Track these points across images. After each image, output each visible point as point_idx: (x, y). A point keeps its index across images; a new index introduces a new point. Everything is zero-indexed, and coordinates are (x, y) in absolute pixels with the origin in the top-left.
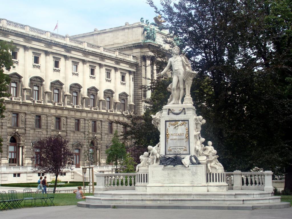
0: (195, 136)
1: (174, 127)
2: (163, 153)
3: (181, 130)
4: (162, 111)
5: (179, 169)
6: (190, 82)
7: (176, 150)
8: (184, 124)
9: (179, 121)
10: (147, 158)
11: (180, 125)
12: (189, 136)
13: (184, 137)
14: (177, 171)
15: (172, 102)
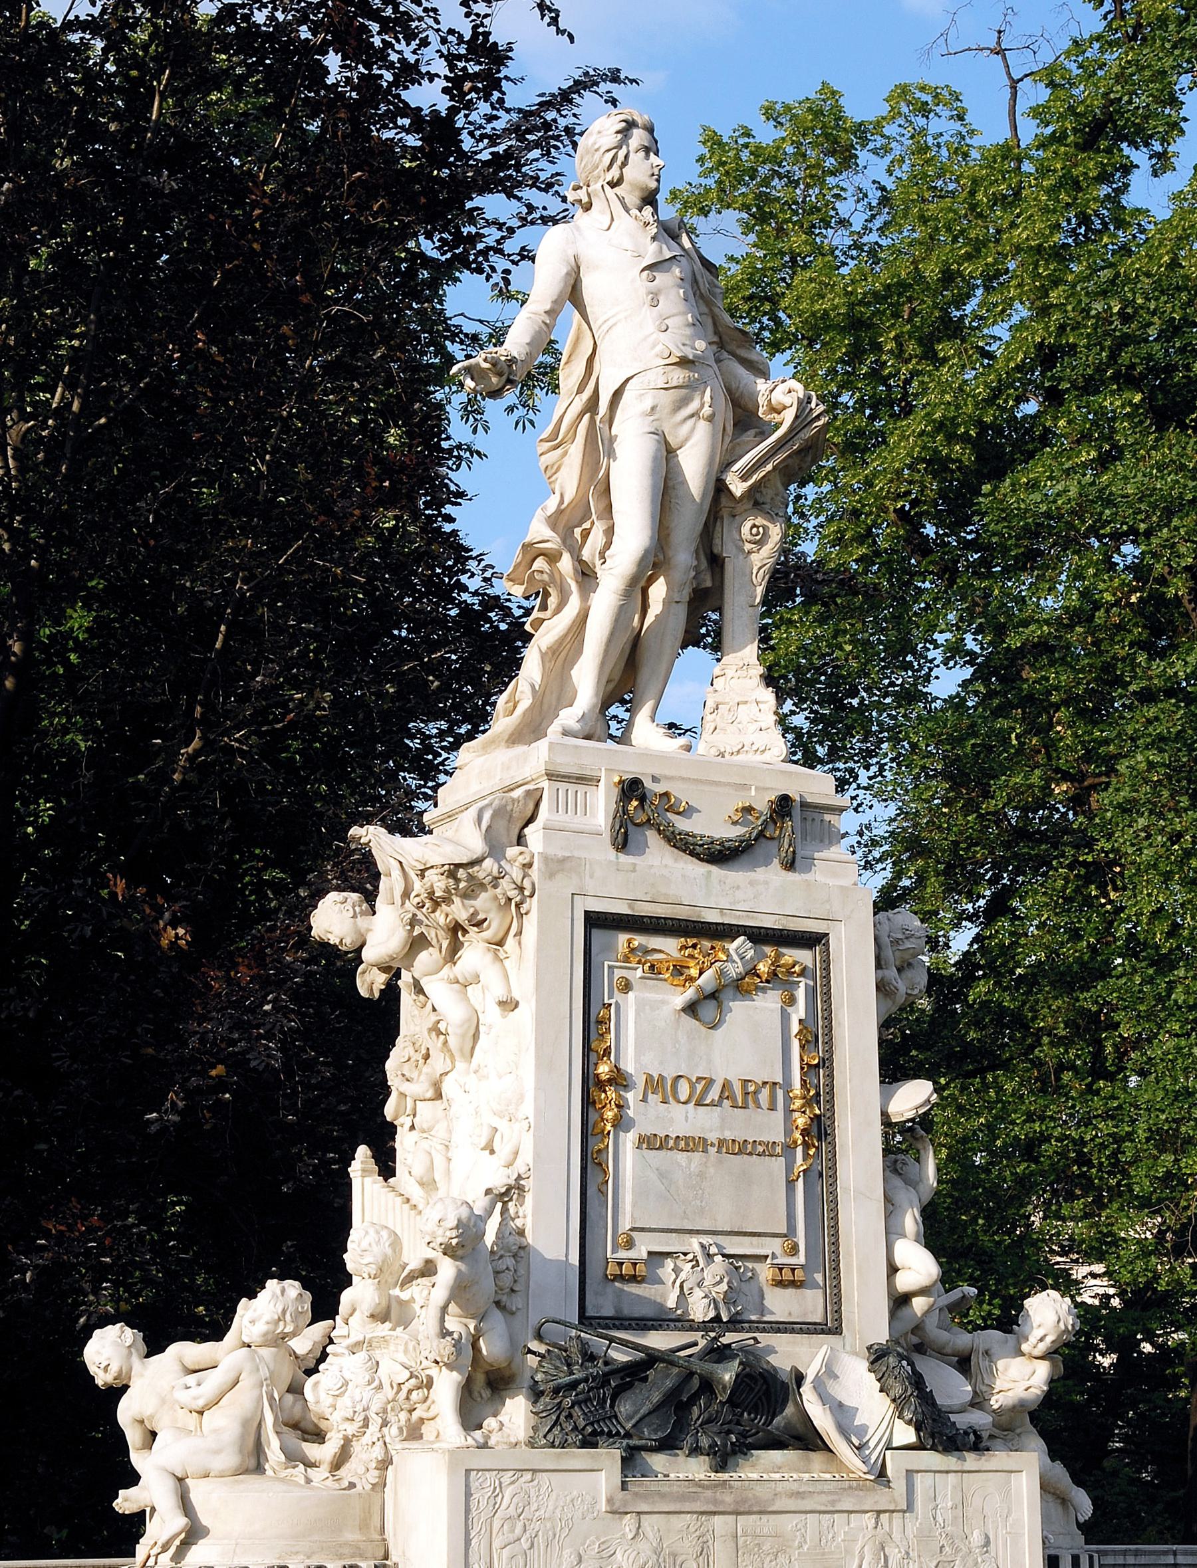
1: (690, 993)
5: (791, 1504)
14: (767, 1524)
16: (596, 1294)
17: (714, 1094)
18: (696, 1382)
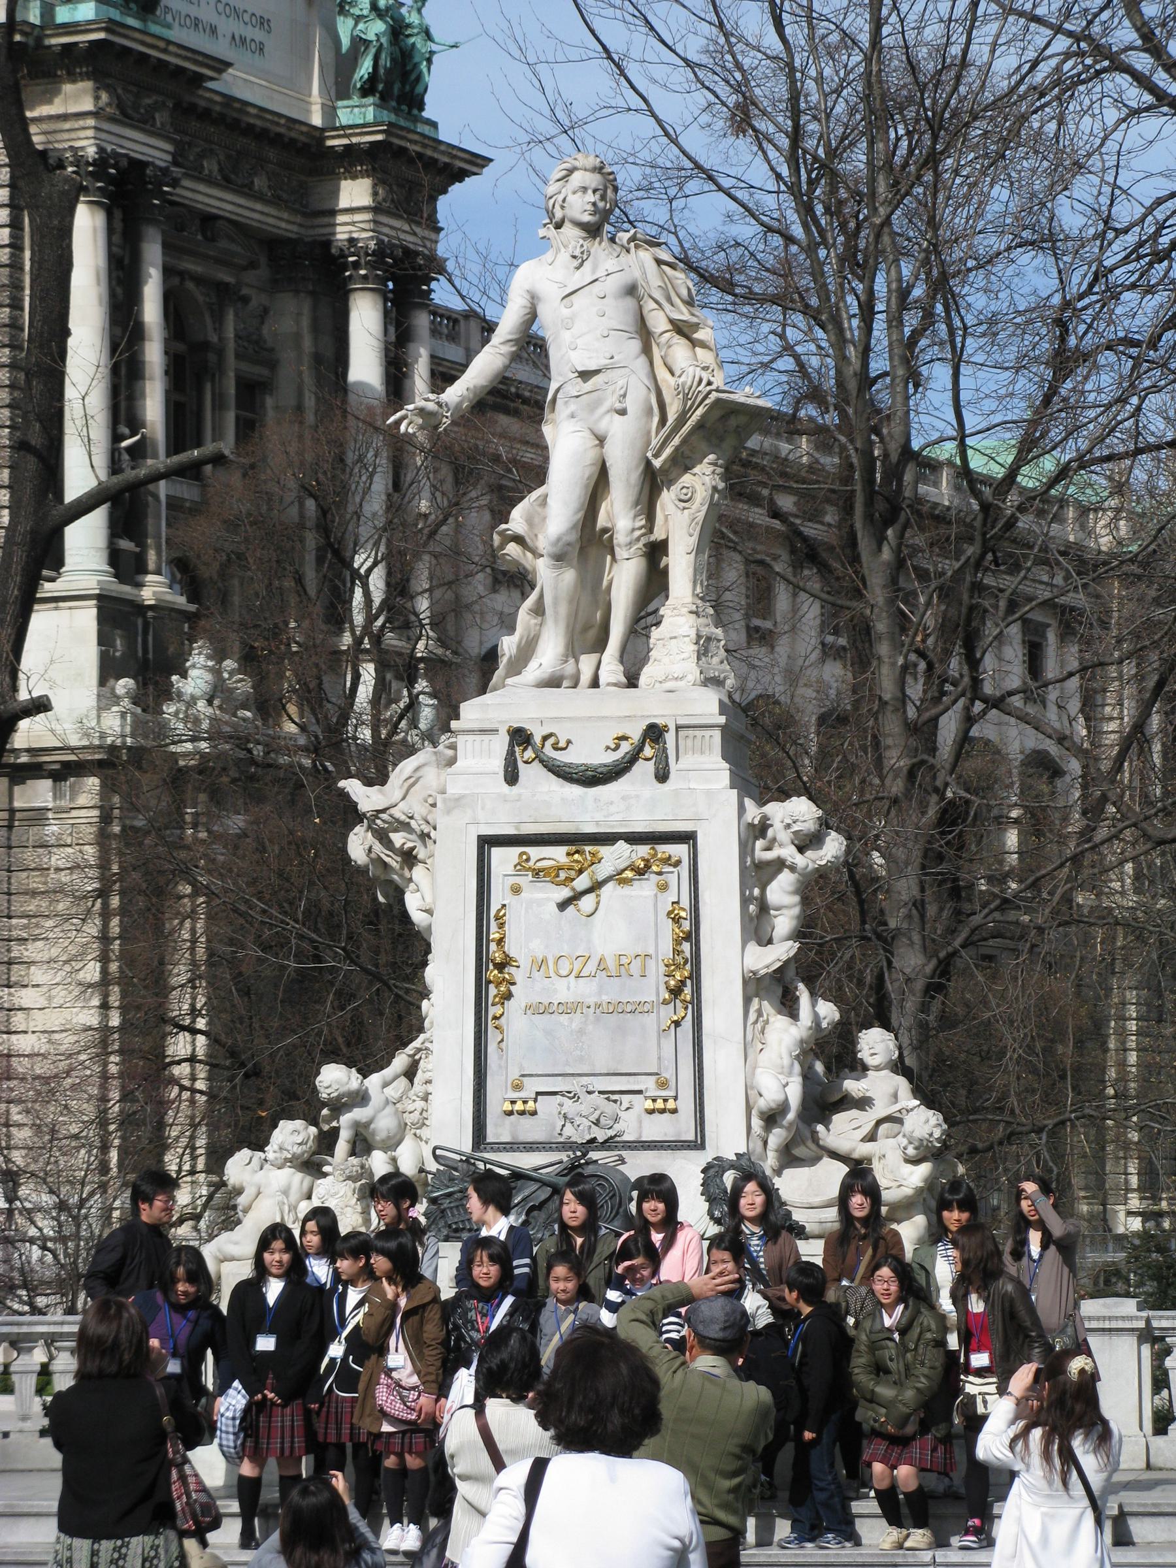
0: (754, 986)
1: (565, 893)
2: (450, 1128)
3: (628, 920)
4: (453, 747)
6: (703, 479)
7: (569, 1106)
8: (648, 866)
9: (608, 839)
10: (297, 1179)
11: (618, 878)
12: (696, 976)
13: (653, 987)
15: (534, 670)
16: (496, 1125)
17: (591, 967)
18: (548, 1191)
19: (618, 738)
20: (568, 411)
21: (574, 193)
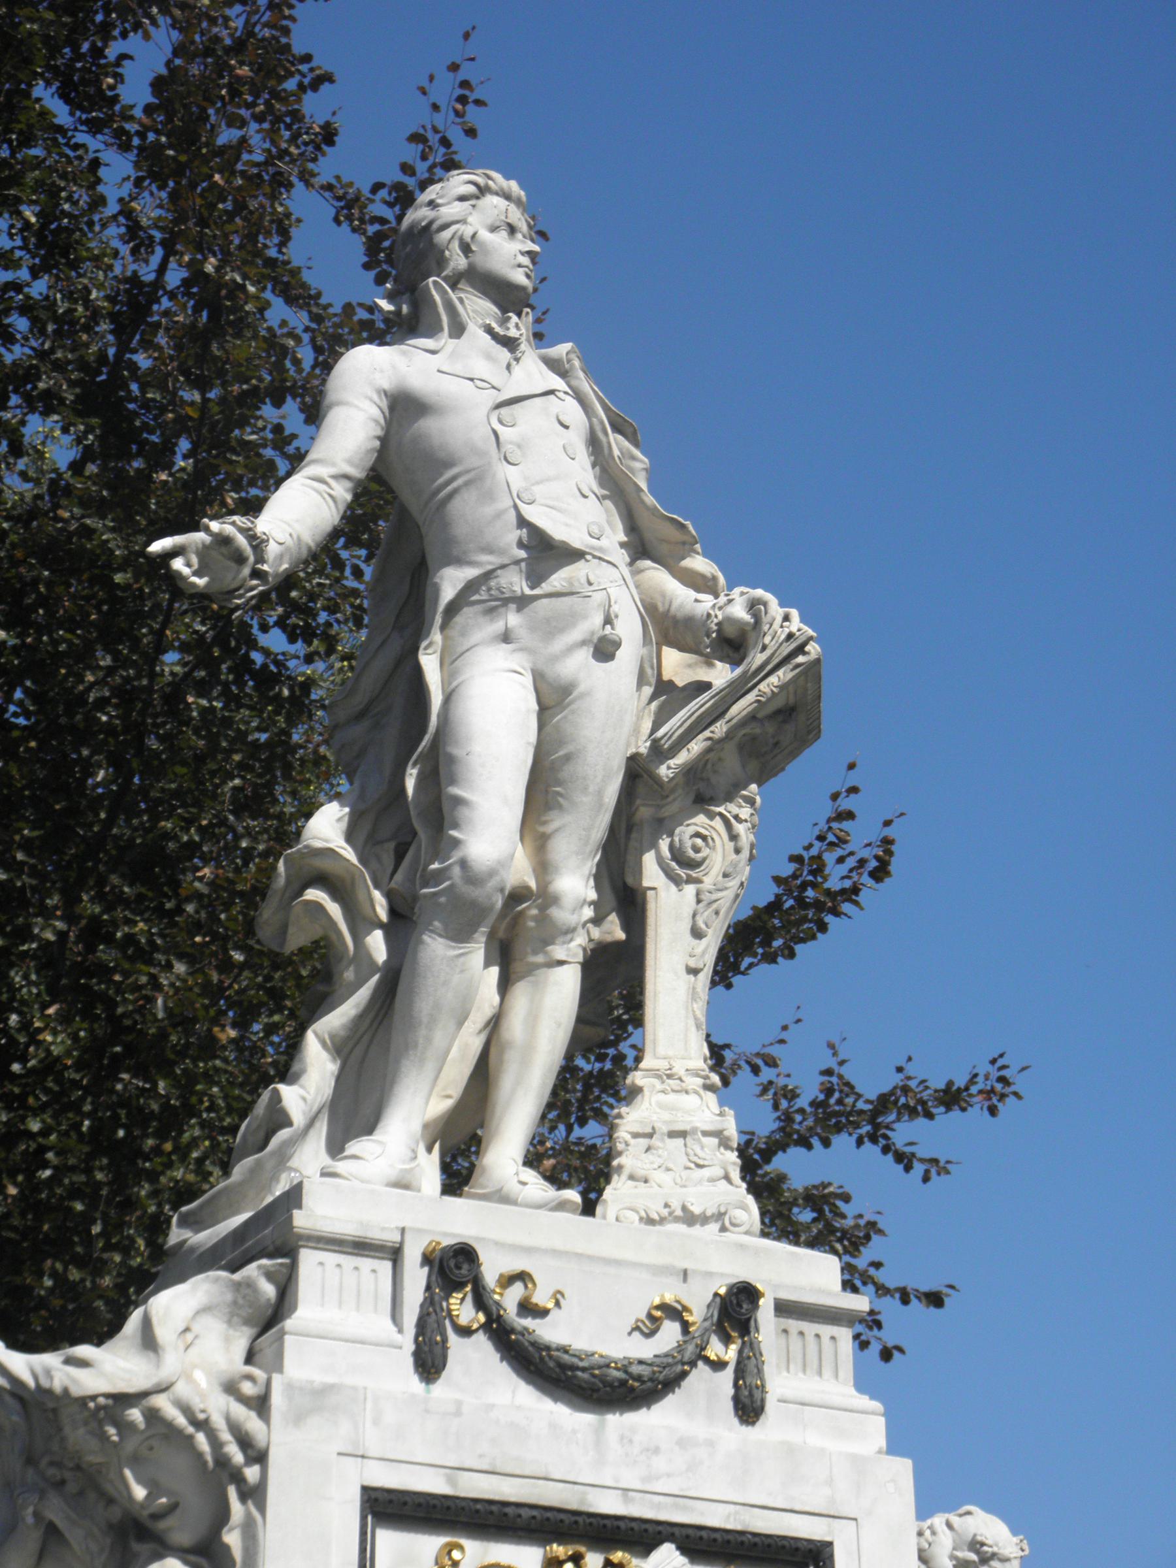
19: (663, 1307)
20: (498, 626)
21: (493, 229)
